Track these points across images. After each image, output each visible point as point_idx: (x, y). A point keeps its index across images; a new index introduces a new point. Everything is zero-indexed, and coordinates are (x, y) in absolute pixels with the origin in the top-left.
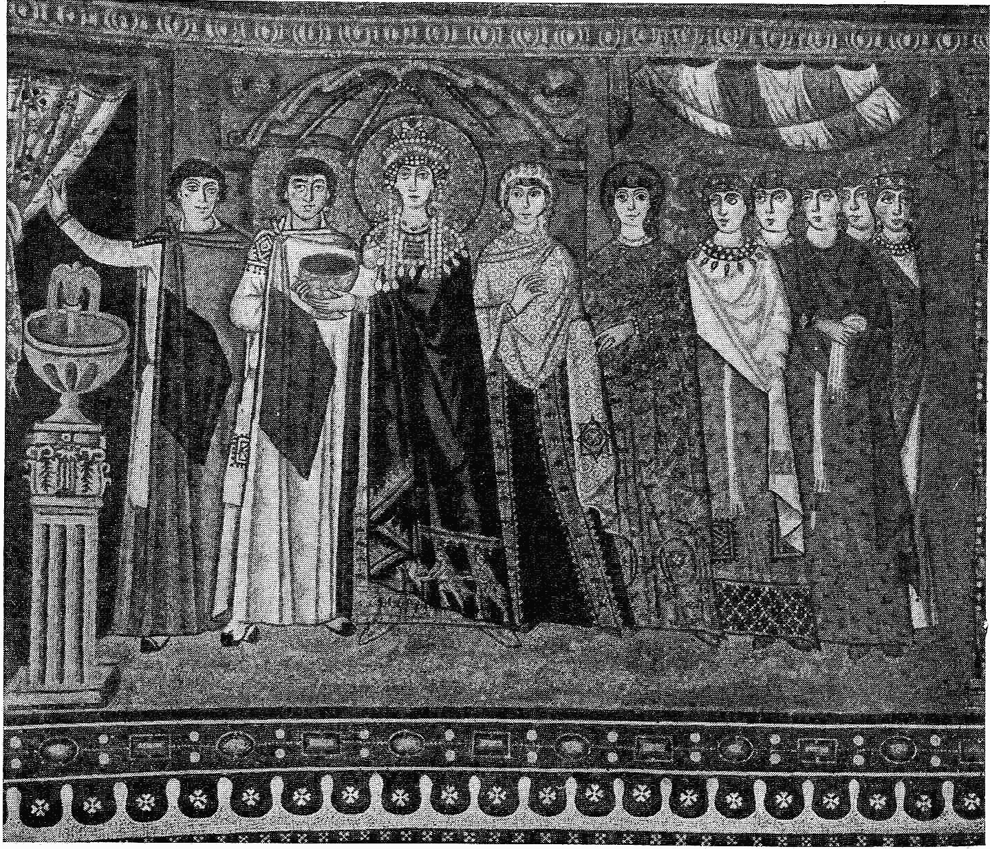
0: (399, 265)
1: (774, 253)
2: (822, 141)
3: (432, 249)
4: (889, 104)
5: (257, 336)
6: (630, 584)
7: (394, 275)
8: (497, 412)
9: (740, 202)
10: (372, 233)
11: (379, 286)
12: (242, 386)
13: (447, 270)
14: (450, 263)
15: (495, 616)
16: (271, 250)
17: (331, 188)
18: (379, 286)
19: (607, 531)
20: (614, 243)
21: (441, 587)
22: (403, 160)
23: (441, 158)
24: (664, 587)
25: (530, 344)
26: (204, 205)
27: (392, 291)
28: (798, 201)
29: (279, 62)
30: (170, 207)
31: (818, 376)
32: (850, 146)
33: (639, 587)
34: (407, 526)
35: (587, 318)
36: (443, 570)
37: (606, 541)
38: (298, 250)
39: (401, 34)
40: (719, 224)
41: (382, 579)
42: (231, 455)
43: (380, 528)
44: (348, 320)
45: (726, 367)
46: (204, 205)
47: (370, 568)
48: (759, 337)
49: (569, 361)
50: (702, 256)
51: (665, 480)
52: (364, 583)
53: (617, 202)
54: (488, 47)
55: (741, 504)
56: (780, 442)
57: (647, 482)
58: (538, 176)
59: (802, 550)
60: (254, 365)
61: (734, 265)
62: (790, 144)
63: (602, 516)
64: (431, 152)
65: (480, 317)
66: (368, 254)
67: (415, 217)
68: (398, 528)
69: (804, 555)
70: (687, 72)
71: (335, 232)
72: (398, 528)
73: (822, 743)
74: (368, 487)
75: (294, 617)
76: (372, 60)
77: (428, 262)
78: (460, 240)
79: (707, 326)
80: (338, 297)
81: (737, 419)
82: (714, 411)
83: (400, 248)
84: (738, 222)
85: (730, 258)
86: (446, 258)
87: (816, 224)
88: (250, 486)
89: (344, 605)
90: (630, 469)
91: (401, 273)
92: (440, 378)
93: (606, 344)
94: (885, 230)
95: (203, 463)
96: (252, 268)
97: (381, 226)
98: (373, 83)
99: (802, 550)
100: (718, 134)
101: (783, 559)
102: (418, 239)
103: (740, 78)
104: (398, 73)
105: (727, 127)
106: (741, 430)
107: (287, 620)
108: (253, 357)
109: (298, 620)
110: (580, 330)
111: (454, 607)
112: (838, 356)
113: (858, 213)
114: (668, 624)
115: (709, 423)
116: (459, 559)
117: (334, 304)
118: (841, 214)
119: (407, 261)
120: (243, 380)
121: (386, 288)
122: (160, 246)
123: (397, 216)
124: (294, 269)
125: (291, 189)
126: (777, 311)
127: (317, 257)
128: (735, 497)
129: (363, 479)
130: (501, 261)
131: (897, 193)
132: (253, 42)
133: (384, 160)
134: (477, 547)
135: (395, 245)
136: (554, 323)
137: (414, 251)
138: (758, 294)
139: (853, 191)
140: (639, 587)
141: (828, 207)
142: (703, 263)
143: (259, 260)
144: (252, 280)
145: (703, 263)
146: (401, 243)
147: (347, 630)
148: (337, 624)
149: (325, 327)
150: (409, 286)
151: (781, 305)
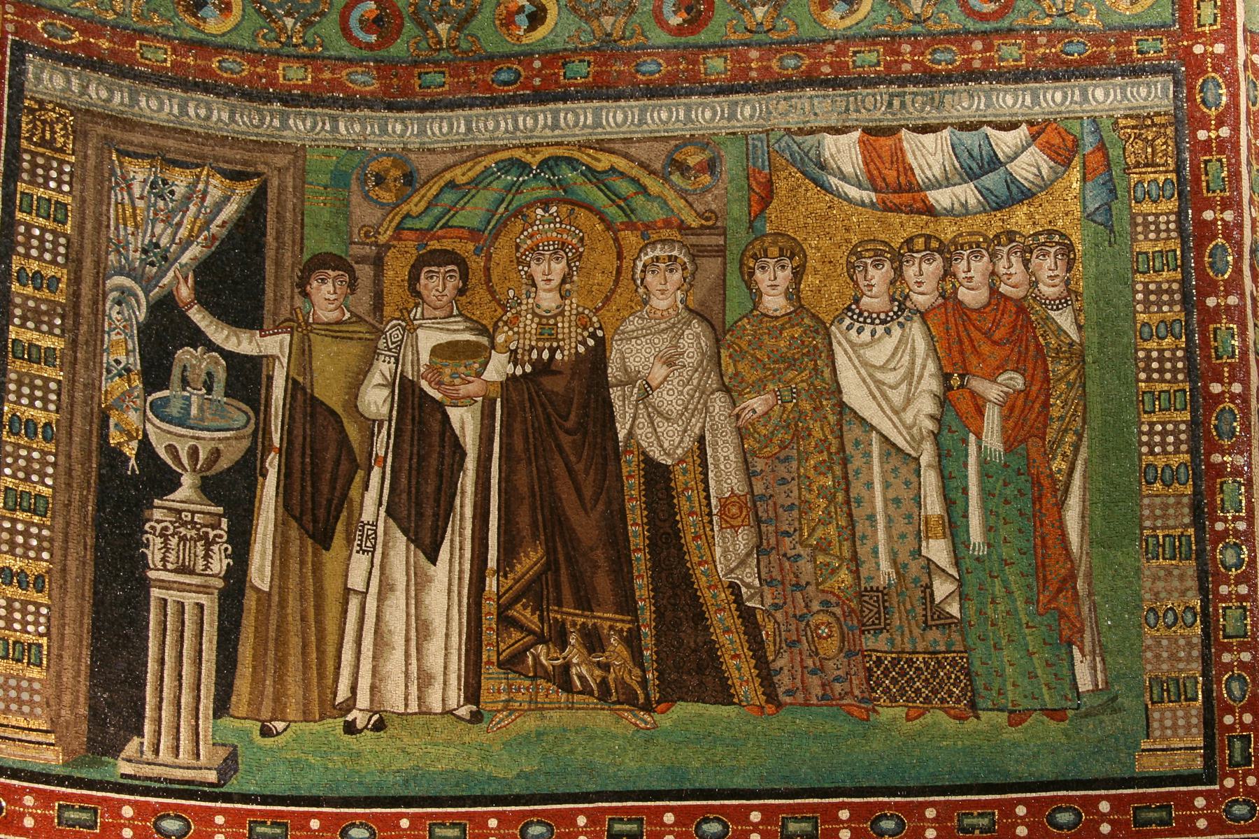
0: (532, 348)
1: (924, 316)
2: (972, 202)
3: (566, 331)
4: (1042, 163)
5: (386, 425)
6: (774, 661)
7: (526, 358)
8: (633, 487)
9: (887, 265)
10: (505, 318)
11: (510, 369)
12: (369, 475)
13: (581, 349)
14: (584, 343)
15: (630, 699)
16: (402, 341)
17: (464, 276)
18: (510, 369)
19: (748, 604)
20: (755, 313)
21: (574, 671)
22: (538, 246)
23: (575, 241)
24: (810, 662)
25: (668, 420)
26: (333, 297)
27: (525, 374)
28: (948, 262)
29: (413, 156)
30: (299, 301)
31: (972, 438)
32: (999, 208)
33: (782, 662)
34: (537, 608)
35: (726, 389)
36: (574, 653)
37: (747, 616)
38: (428, 339)
39: (536, 120)
40: (865, 289)
41: (513, 664)
42: (357, 542)
43: (510, 613)
44: (478, 406)
45: (874, 434)
46: (333, 297)
47: (499, 654)
48: (908, 401)
49: (708, 437)
50: (847, 321)
51: (809, 550)
52: (494, 669)
53: (758, 274)
54: (624, 129)
55: (892, 571)
56: (933, 505)
57: (791, 553)
58: (675, 253)
59: (958, 616)
60: (382, 453)
61: (880, 329)
62: (938, 208)
63: (744, 590)
64: (565, 236)
65: (615, 394)
66: (500, 339)
67: (548, 300)
68: (529, 609)
69: (961, 621)
70: (829, 139)
71: (467, 319)
72: (529, 609)
73: (980, 815)
74: (498, 571)
75: (419, 706)
76: (506, 148)
77: (561, 343)
78: (595, 319)
79: (855, 393)
80: (469, 382)
81: (886, 485)
82: (863, 478)
83: (533, 331)
84: (884, 288)
85: (877, 321)
86: (580, 338)
87: (965, 283)
88: (376, 572)
89: (472, 693)
90: (773, 541)
91: (534, 355)
92: (573, 458)
93: (747, 415)
94: (1041, 286)
95: (327, 549)
96: (382, 358)
97: (514, 311)
98: (507, 173)
99: (958, 616)
100: (863, 202)
101: (937, 626)
102: (552, 321)
103: (886, 142)
104: (534, 160)
105: (873, 195)
106: (891, 494)
107: (414, 707)
108: (381, 444)
109: (424, 709)
110: (719, 403)
111: (587, 691)
112: (992, 418)
113: (1012, 270)
114: (814, 701)
115: (857, 489)
116: (593, 642)
117: (464, 390)
118: (993, 273)
119: (540, 344)
120: (370, 469)
121: (519, 371)
122: (287, 337)
123: (531, 301)
124: (425, 358)
125: (423, 281)
126: (926, 374)
127: (450, 344)
128: (885, 565)
129: (492, 563)
130: (637, 338)
131: (1052, 250)
132: (385, 138)
133: (518, 247)
134: (611, 628)
135: (528, 329)
136: (692, 397)
137: (547, 329)
138: (906, 358)
139: (1006, 249)
140: (782, 662)
141: (979, 267)
142: (849, 328)
143: (390, 350)
144: (383, 367)
145: (849, 328)
146: (534, 326)
147: (476, 717)
148: (464, 712)
149: (454, 414)
150: (544, 368)
151: (931, 367)
